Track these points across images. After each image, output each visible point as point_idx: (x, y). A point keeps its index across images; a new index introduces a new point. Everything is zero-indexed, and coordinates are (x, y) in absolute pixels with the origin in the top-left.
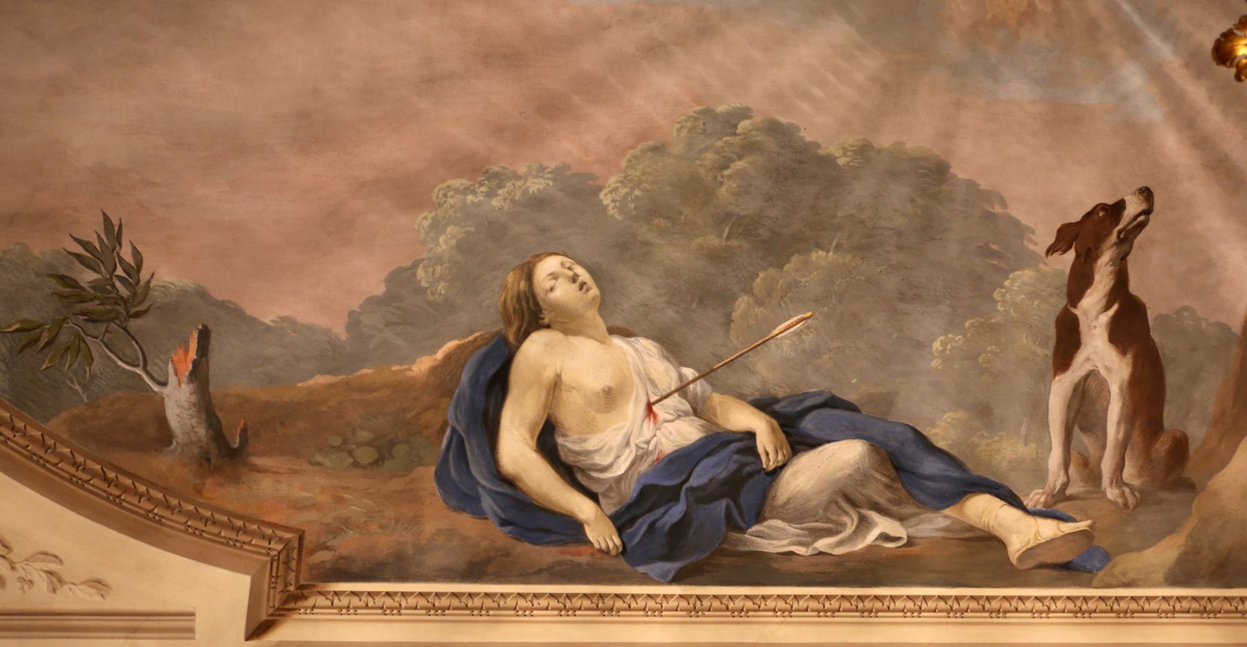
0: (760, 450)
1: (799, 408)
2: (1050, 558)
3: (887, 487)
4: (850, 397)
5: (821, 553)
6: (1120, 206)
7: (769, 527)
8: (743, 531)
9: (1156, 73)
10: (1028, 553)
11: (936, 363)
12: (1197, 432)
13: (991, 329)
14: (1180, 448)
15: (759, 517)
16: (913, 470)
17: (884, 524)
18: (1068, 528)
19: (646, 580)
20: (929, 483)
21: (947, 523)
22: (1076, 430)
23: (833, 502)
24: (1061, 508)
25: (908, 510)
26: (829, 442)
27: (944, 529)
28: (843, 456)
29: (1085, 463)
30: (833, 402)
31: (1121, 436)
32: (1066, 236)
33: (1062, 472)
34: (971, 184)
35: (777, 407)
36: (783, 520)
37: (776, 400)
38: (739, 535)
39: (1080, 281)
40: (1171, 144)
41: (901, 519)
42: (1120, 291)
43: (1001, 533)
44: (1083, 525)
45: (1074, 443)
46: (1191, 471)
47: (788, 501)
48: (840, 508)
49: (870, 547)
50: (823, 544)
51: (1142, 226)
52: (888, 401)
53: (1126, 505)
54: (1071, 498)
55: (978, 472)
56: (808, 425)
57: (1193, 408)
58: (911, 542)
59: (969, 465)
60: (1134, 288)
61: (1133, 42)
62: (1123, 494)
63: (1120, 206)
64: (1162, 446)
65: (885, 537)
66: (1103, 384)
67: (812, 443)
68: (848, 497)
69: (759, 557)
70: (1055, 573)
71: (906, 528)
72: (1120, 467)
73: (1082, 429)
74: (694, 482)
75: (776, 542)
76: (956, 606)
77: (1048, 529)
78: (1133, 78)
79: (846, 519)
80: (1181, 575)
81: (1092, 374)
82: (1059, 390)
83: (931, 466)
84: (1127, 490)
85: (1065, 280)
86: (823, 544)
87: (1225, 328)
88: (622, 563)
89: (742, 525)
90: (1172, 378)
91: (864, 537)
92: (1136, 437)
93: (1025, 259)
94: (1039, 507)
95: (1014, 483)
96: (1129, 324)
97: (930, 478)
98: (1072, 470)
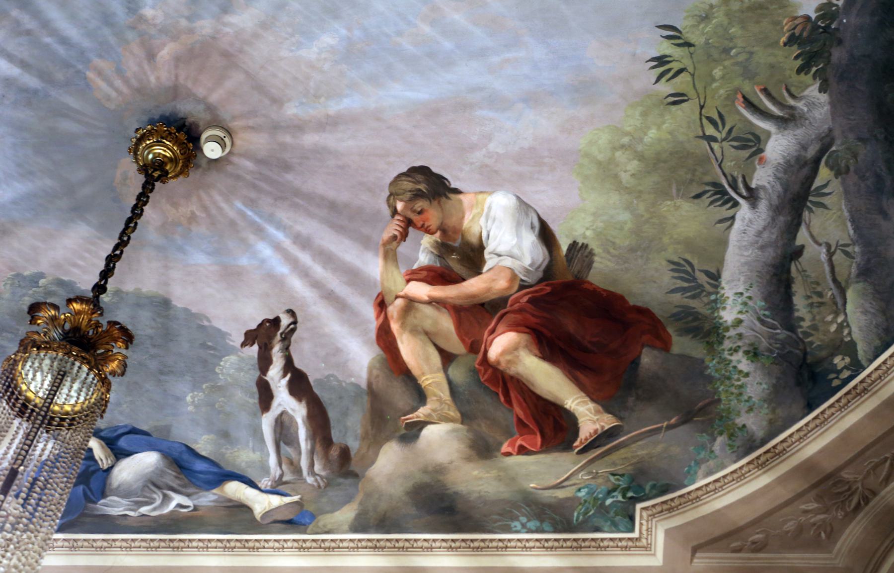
0: (97, 457)
1: (115, 434)
2: (280, 517)
3: (176, 477)
4: (144, 428)
5: (143, 515)
6: (276, 321)
7: (111, 501)
8: (95, 503)
9: (278, 247)
10: (266, 514)
11: (190, 408)
12: (354, 445)
13: (217, 389)
14: (345, 454)
15: (103, 495)
16: (187, 467)
17: (177, 499)
18: (287, 500)
20: (201, 476)
21: (215, 497)
22: (282, 444)
23: (145, 486)
24: (281, 488)
25: (191, 490)
26: (137, 453)
27: (214, 501)
28: (146, 461)
29: (291, 463)
30: (134, 431)
31: (309, 447)
32: (250, 337)
33: (278, 468)
34: (186, 310)
35: (102, 434)
36: (118, 496)
37: (102, 431)
38: (92, 505)
39: (265, 362)
40: (297, 285)
41: (188, 495)
42: (289, 366)
43: (249, 503)
44: (296, 498)
45: (282, 452)
46: (354, 466)
47: (119, 486)
48: (151, 490)
49: (172, 512)
50: (144, 510)
51: (293, 331)
52: (167, 429)
53: (319, 486)
54: (286, 483)
55: (229, 468)
56: (123, 443)
57: (349, 428)
58: (196, 508)
59: (222, 464)
60: (298, 364)
61: (259, 231)
62: (316, 480)
63: (276, 321)
64: (334, 453)
65: (180, 506)
66: (292, 418)
67: (128, 454)
68: (154, 483)
69: (106, 517)
70: (283, 526)
71: (192, 500)
72: (312, 465)
73: (286, 444)
75: (116, 509)
76: (228, 545)
77: (276, 501)
78: (265, 251)
79: (155, 496)
80: (359, 526)
81: (283, 413)
82: (267, 422)
83: (200, 466)
84: (318, 478)
85: (256, 361)
86: (144, 510)
87: (357, 386)
89: (94, 499)
90: (332, 414)
91: (168, 505)
92: (318, 448)
93: (230, 351)
94: (268, 488)
95: (251, 474)
96: (299, 385)
97: (201, 472)
98: (284, 467)
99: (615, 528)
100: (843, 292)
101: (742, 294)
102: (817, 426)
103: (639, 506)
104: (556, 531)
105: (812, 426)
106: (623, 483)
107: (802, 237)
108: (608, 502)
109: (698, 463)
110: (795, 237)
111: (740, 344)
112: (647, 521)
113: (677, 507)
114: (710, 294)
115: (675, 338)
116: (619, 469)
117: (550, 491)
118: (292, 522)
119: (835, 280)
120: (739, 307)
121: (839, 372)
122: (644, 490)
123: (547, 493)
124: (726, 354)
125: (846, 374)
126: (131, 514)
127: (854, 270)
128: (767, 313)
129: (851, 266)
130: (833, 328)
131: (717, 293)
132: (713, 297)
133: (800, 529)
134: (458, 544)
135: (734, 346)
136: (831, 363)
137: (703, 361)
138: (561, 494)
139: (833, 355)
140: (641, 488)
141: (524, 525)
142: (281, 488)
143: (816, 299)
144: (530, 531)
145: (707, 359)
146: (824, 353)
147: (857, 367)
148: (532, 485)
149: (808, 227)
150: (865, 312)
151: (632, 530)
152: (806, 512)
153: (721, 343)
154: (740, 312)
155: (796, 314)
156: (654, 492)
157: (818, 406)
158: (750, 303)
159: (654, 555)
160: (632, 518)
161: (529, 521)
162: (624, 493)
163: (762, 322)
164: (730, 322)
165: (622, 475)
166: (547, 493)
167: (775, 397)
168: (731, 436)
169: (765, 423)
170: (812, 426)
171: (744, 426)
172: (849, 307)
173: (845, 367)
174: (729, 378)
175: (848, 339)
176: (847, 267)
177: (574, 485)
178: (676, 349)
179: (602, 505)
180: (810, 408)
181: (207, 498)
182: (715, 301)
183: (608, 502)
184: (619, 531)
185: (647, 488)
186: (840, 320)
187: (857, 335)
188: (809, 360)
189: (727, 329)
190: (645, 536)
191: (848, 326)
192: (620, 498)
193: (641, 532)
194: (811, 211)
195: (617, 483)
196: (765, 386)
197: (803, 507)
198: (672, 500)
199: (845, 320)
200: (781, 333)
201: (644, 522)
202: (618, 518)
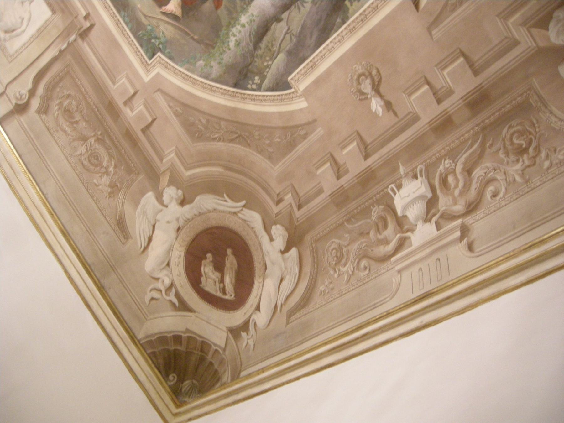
99: (146, 52)
100: (279, 52)
101: (253, 16)
102: (231, 95)
103: (159, 54)
104: (131, 30)
105: (230, 93)
106: (163, 40)
107: (285, 16)
108: (153, 41)
109: (188, 62)
110: (283, 12)
111: (238, 35)
114: (245, 3)
115: (223, 7)
116: (166, 33)
119: (280, 45)
120: (248, 20)
121: (253, 83)
122: (166, 50)
123: (140, 14)
124: (231, 33)
125: (254, 87)
127: (287, 48)
128: (254, 33)
129: (288, 45)
130: (265, 64)
131: (247, 6)
132: (245, 6)
133: (193, 124)
135: (235, 33)
136: (254, 77)
137: (222, 27)
138: (143, 20)
139: (257, 74)
140: (165, 48)
141: (124, 16)
143: (270, 46)
144: (124, 21)
145: (224, 28)
146: (255, 70)
147: (259, 89)
149: (290, 13)
150: (278, 69)
151: (150, 59)
152: (200, 121)
153: (233, 27)
154: (247, 23)
155: (261, 45)
157: (238, 88)
158: (253, 22)
160: (154, 55)
163: (250, 35)
164: (241, 23)
165: (165, 37)
166: (140, 14)
167: (230, 68)
168: (206, 65)
169: (218, 74)
170: (230, 93)
171: (212, 67)
172: (276, 61)
173: (257, 84)
174: (224, 43)
175: (265, 73)
176: (287, 45)
178: (219, 11)
179: (151, 39)
180: (236, 86)
182: (244, 9)
184: (146, 54)
185: (167, 51)
186: (270, 63)
187: (269, 76)
188: (250, 67)
189: (239, 24)
191: (270, 68)
192: (157, 44)
193: (151, 63)
194: (295, 7)
196: (230, 61)
197: (201, 118)
199: (271, 65)
200: (251, 47)
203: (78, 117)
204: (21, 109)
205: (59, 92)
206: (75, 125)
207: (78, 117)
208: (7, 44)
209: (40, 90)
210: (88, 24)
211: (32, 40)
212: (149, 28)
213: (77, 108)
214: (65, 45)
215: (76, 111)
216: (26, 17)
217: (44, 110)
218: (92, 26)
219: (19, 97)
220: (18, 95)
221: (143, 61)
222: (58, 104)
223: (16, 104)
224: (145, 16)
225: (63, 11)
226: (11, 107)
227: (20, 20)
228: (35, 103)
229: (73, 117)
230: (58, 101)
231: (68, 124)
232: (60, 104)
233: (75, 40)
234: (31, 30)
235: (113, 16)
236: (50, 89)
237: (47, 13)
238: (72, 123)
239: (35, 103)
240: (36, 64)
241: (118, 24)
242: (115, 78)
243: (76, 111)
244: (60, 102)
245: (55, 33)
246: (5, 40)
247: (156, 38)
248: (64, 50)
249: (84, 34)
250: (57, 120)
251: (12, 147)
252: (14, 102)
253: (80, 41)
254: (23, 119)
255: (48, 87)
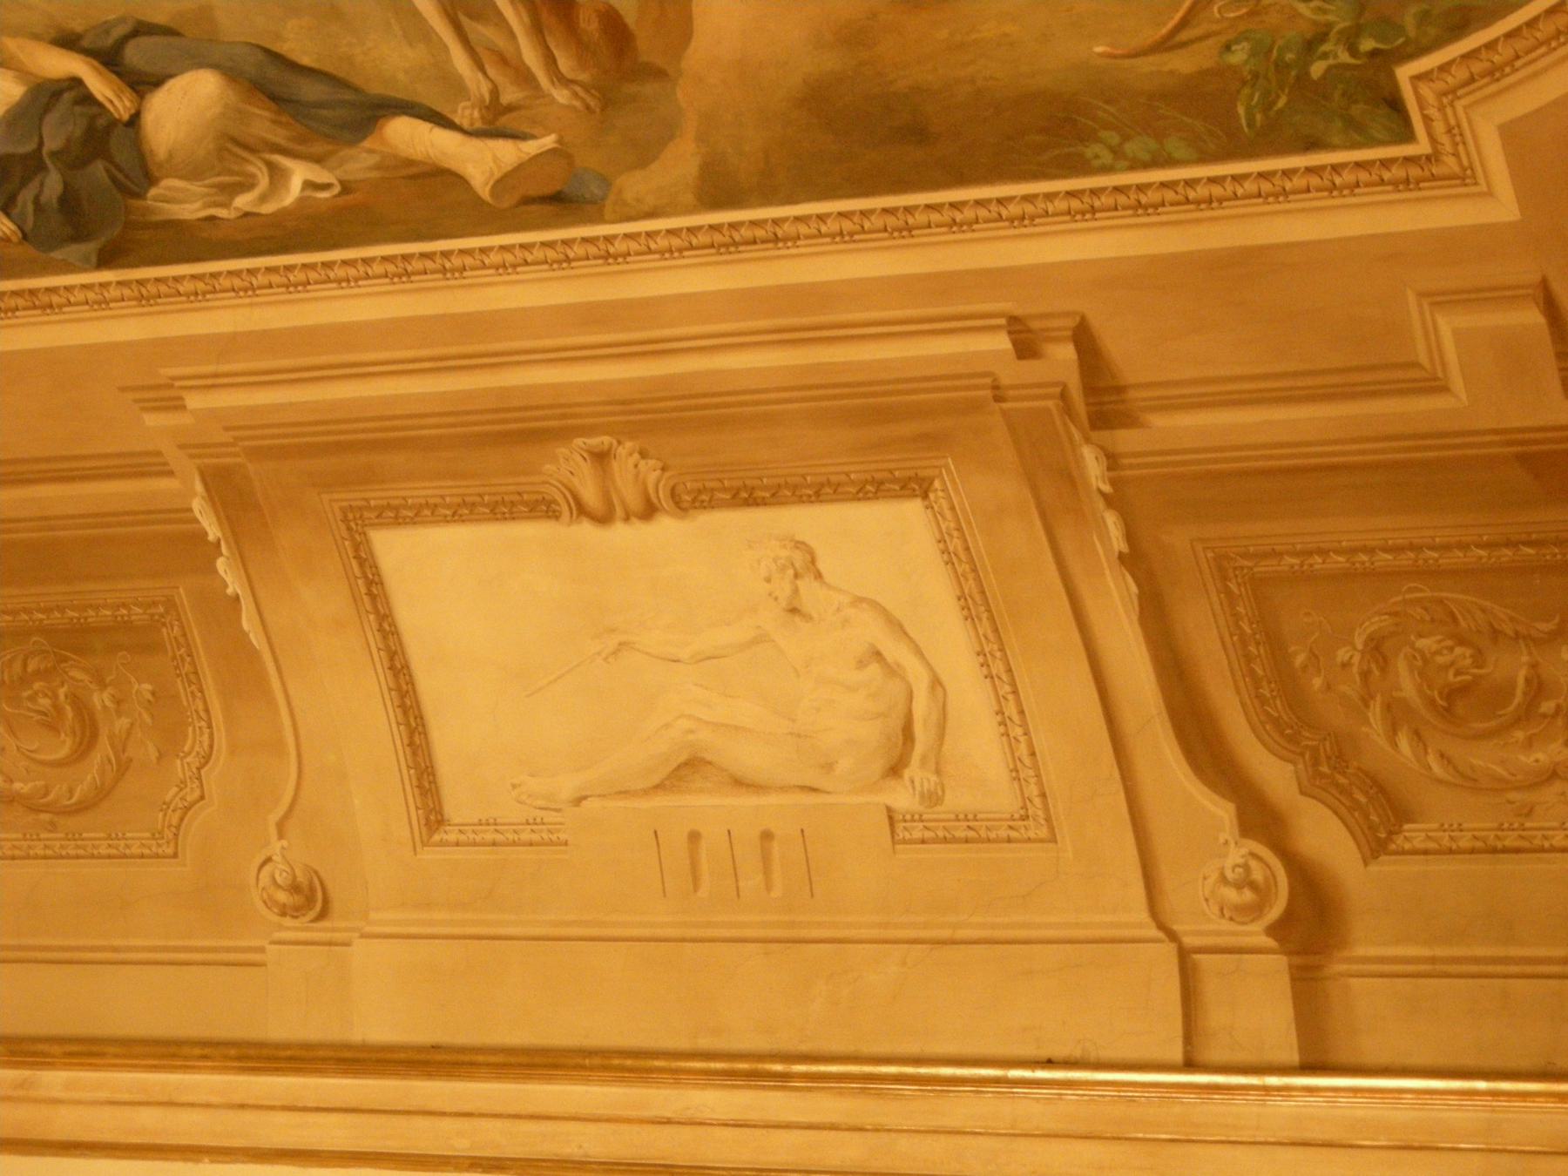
0: (100, 97)
3: (274, 122)
4: (159, 18)
5: (247, 214)
7: (169, 188)
8: (140, 196)
10: (502, 184)
15: (151, 180)
17: (299, 174)
18: (531, 148)
19: (67, 268)
20: (324, 112)
21: (372, 160)
22: (464, 20)
24: (504, 121)
25: (319, 148)
26: (171, 76)
27: (377, 167)
29: (503, 60)
30: (142, 29)
31: (526, 19)
33: (480, 75)
35: (85, 43)
36: (181, 178)
37: (79, 37)
38: (139, 203)
41: (319, 160)
44: (549, 141)
45: (471, 36)
46: (647, 48)
47: (171, 155)
48: (238, 156)
49: (301, 200)
50: (243, 201)
53: (588, 107)
54: (510, 108)
55: (376, 89)
56: (134, 55)
58: (346, 188)
59: (357, 80)
62: (576, 95)
64: (589, 24)
67: (157, 82)
69: (176, 226)
70: (547, 209)
71: (331, 170)
72: (550, 60)
73: (475, 16)
74: (52, 143)
75: (187, 206)
77: (507, 153)
79: (251, 169)
83: (311, 91)
84: (578, 89)
88: (29, 251)
89: (136, 189)
91: (288, 190)
92: (548, 18)
94: (478, 125)
97: (320, 105)
98: (491, 71)
99: (1359, 134)
103: (1404, 73)
104: (1204, 158)
108: (1317, 69)
112: (1441, 109)
113: (1510, 63)
117: (1151, 59)
118: (557, 198)
122: (1401, 30)
126: (222, 213)
134: (969, 214)
138: (1182, 63)
141: (1117, 152)
142: (504, 121)
144: (1136, 165)
148: (1099, 49)
151: (1408, 136)
156: (1432, 31)
159: (1489, 194)
160: (1395, 104)
161: (1126, 138)
162: (1350, 40)
166: (1147, 65)
177: (1207, 36)
179: (1303, 77)
181: (359, 162)
183: (1317, 69)
185: (1409, 22)
190: (1448, 148)
192: (1344, 57)
193: (1433, 139)
195: (1321, 18)
198: (1491, 46)
201: (1433, 112)
202: (1357, 110)
203: (1512, 666)
204: (1310, 923)
205: (1328, 687)
206: (1547, 706)
207: (1512, 666)
208: (958, 799)
209: (1275, 775)
210: (1065, 353)
211: (998, 667)
212: (1239, 56)
213: (1462, 642)
214: (1111, 520)
215: (1479, 659)
216: (870, 630)
217: (1382, 816)
218: (1084, 339)
219: (1248, 896)
220: (1231, 895)
221: (1398, 172)
222: (1393, 730)
223: (1273, 930)
224: (1165, 45)
225: (934, 441)
226: (1279, 963)
227: (874, 669)
228: (1325, 836)
229: (1502, 694)
230: (1375, 713)
231: (1519, 735)
232: (1396, 714)
233: (1112, 460)
234: (952, 645)
235: (1087, 210)
236: (1293, 723)
237: (906, 518)
238: (1527, 714)
239: (1325, 836)
240: (1130, 722)
241: (1140, 205)
242: (1416, 365)
243: (1479, 659)
244: (1388, 707)
245: (1024, 539)
246: (933, 798)
247: (1311, 46)
248: (1130, 536)
249: (1104, 399)
250: (1469, 782)
251: (1481, 1085)
252: (1255, 933)
253: (1126, 440)
254: (1368, 941)
255: (1276, 722)
